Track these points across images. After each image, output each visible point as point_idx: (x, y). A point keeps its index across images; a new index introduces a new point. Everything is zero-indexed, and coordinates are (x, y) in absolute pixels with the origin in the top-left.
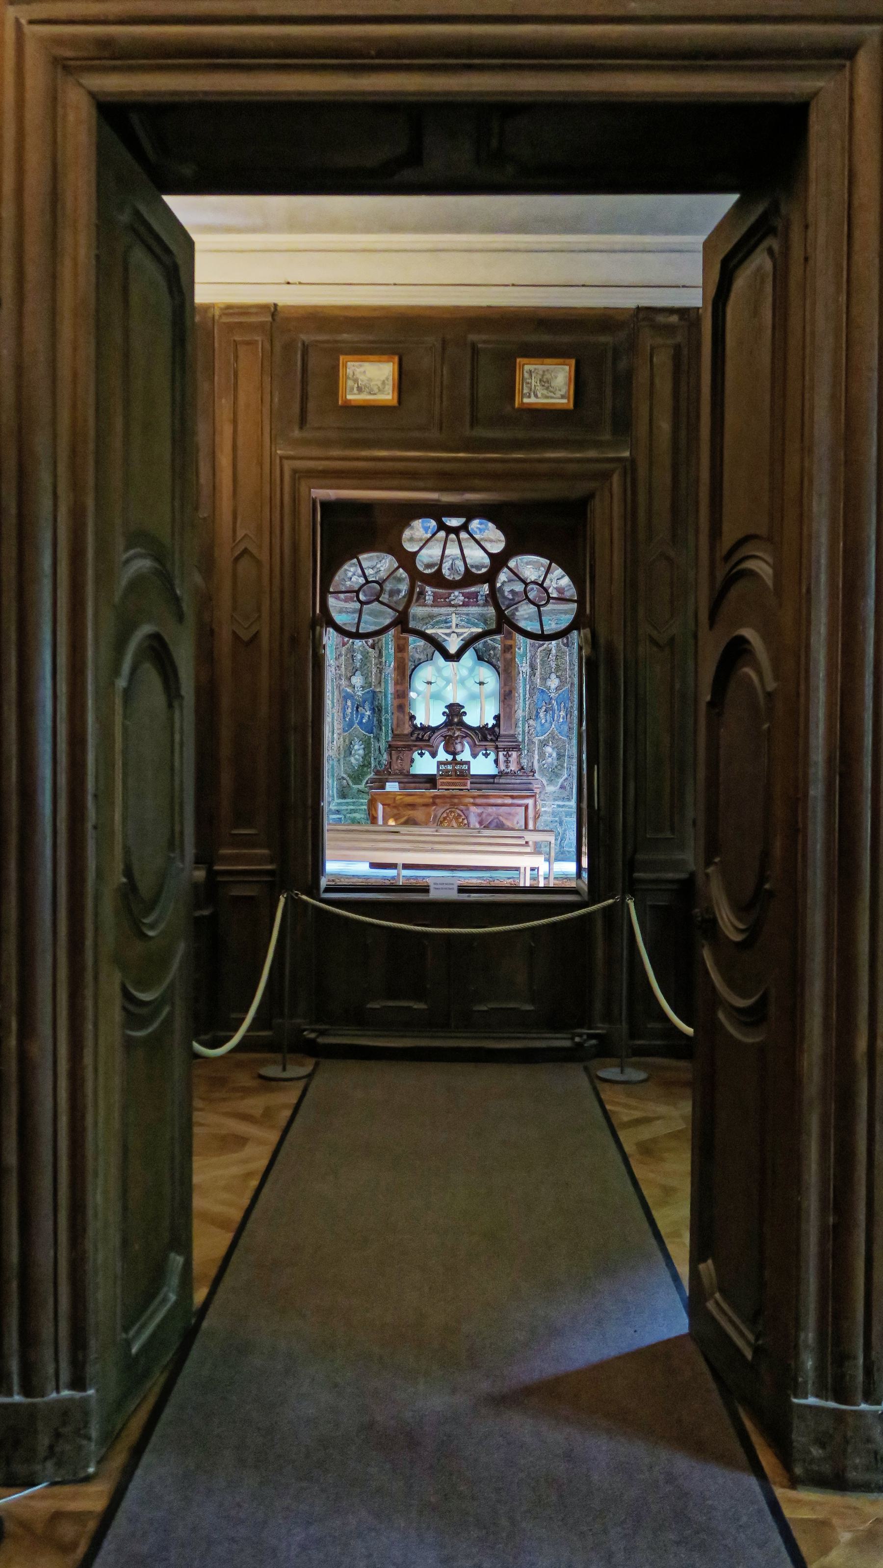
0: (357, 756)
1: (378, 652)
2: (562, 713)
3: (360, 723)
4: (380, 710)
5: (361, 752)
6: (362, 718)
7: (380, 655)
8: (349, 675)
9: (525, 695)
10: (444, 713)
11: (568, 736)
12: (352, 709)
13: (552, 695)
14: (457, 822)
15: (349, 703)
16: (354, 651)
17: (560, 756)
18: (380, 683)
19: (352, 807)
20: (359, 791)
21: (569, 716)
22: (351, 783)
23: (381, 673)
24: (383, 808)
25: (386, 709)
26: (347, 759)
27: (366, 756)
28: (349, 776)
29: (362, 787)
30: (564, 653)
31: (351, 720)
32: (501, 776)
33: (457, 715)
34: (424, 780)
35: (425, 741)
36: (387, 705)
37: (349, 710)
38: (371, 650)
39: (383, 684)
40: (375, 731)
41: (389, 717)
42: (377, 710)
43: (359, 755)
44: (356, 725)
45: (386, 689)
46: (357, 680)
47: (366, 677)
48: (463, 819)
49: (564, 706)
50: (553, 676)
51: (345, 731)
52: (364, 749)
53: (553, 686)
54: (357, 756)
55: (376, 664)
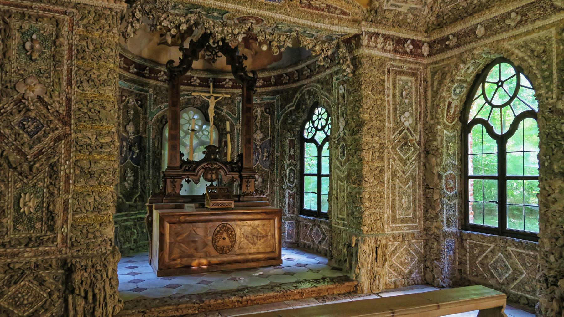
0: (129, 182)
1: (144, 110)
2: (266, 154)
3: (132, 158)
4: (145, 150)
5: (132, 178)
6: (133, 155)
7: (145, 113)
8: (125, 124)
9: (238, 143)
10: (204, 152)
11: (270, 168)
12: (127, 148)
13: (257, 143)
14: (227, 234)
15: (125, 144)
16: (129, 108)
17: (264, 181)
18: (145, 131)
19: (126, 218)
20: (130, 206)
21: (271, 156)
22: (125, 201)
23: (146, 125)
24: (170, 227)
25: (149, 149)
26: (123, 183)
27: (135, 182)
28: (124, 195)
29: (132, 203)
30: (267, 118)
31: (126, 155)
32: (244, 196)
33: (214, 154)
34: (189, 200)
35: (191, 171)
36: (149, 146)
37: (125, 149)
38: (139, 108)
39: (147, 132)
40: (141, 164)
41: (151, 154)
42: (142, 149)
43: (130, 180)
44: (129, 160)
45: (149, 135)
46: (131, 128)
47: (137, 125)
48: (232, 231)
49: (267, 150)
50: (258, 132)
51: (122, 164)
52: (134, 176)
53: (258, 138)
54: (129, 182)
55: (143, 119)
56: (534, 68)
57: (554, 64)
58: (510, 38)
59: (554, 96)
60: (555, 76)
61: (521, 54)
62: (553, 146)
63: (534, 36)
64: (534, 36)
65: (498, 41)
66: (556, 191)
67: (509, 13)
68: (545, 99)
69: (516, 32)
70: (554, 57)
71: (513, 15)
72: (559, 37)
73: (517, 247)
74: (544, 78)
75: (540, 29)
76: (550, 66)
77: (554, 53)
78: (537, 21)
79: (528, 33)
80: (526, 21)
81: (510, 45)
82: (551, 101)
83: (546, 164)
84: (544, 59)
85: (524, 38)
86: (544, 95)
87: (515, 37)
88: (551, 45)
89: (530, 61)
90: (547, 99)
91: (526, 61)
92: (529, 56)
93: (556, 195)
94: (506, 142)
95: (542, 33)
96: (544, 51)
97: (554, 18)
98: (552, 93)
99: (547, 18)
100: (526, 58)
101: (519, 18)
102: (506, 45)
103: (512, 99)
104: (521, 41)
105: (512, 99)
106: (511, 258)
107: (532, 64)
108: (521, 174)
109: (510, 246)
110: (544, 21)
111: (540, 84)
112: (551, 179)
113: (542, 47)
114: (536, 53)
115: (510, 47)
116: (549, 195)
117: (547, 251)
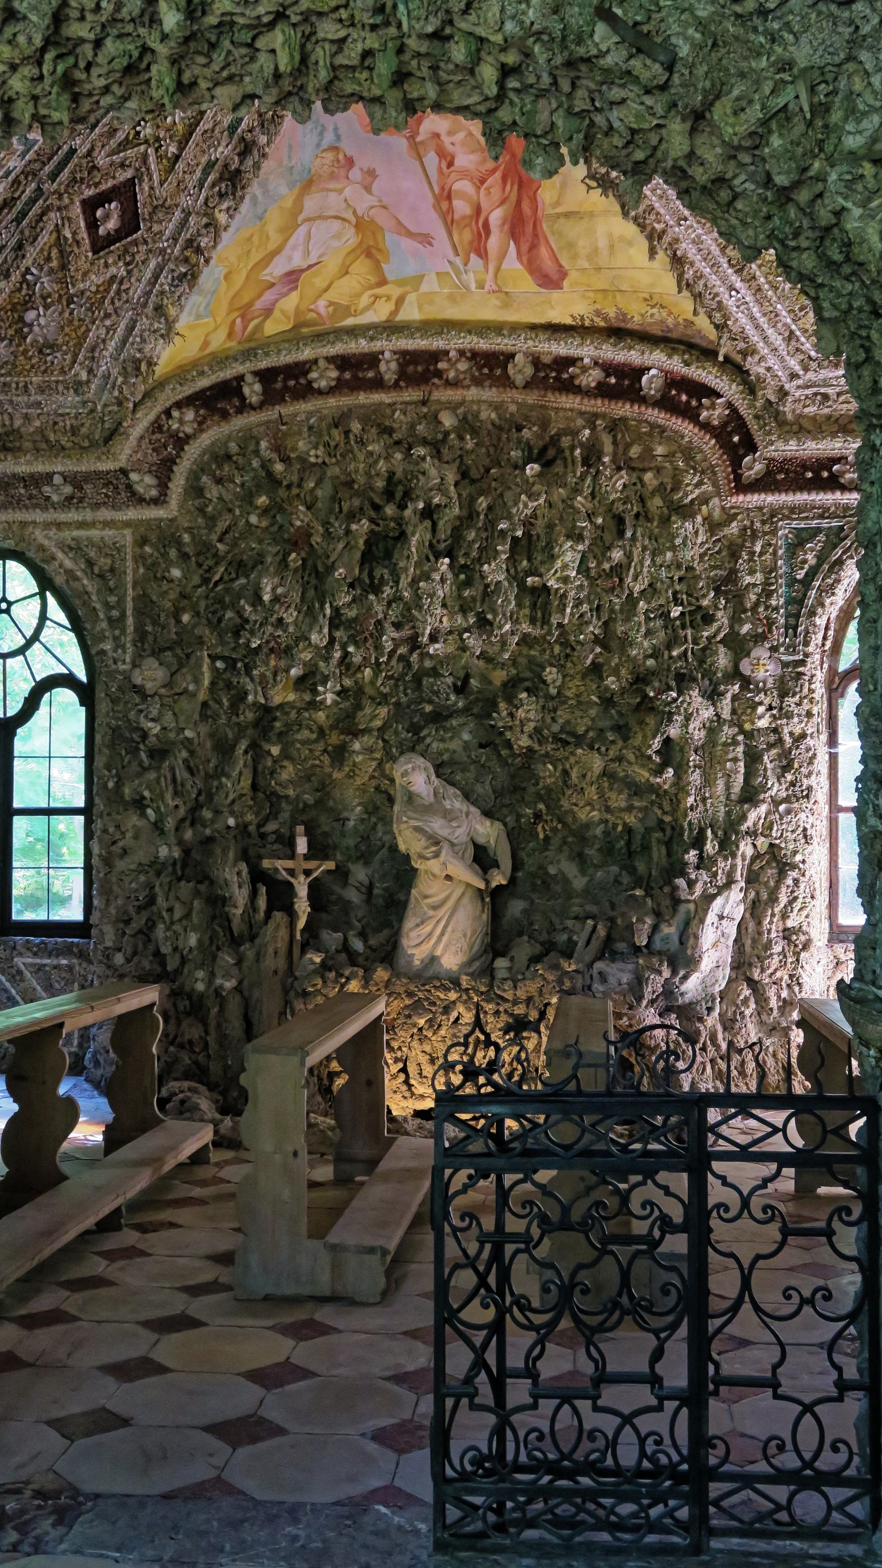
56: (94, 598)
57: (129, 599)
58: (47, 525)
59: (128, 660)
60: (130, 621)
61: (68, 564)
62: (123, 753)
63: (94, 533)
64: (95, 533)
65: (24, 524)
66: (129, 835)
67: (49, 476)
68: (111, 662)
69: (63, 517)
70: (129, 586)
71: (57, 480)
72: (138, 550)
73: (35, 954)
74: (110, 620)
75: (108, 524)
76: (121, 603)
77: (129, 578)
78: (103, 509)
79: (82, 525)
80: (81, 500)
81: (46, 537)
82: (122, 667)
83: (111, 784)
84: (111, 583)
85: (76, 533)
86: (110, 654)
87: (59, 525)
88: (124, 560)
89: (85, 582)
90: (115, 663)
91: (77, 579)
92: (84, 571)
93: (128, 840)
94: (14, 734)
95: (108, 533)
96: (112, 570)
97: (132, 514)
98: (124, 652)
99: (120, 509)
100: (79, 574)
101: (68, 490)
102: (39, 535)
103: (29, 643)
104: (67, 535)
105: (29, 643)
106: (22, 980)
107: (90, 589)
108: (43, 805)
109: (21, 954)
110: (113, 513)
111: (103, 630)
112: (118, 813)
113: (109, 561)
114: (96, 570)
115: (46, 543)
116: (114, 843)
117: (107, 948)
